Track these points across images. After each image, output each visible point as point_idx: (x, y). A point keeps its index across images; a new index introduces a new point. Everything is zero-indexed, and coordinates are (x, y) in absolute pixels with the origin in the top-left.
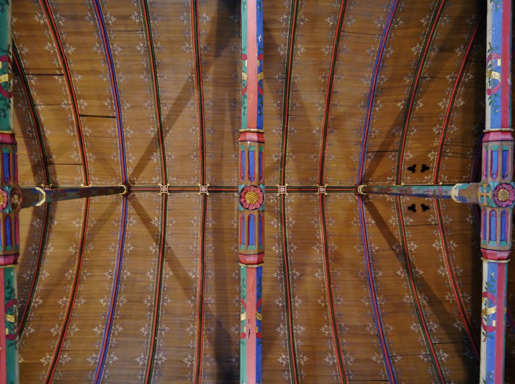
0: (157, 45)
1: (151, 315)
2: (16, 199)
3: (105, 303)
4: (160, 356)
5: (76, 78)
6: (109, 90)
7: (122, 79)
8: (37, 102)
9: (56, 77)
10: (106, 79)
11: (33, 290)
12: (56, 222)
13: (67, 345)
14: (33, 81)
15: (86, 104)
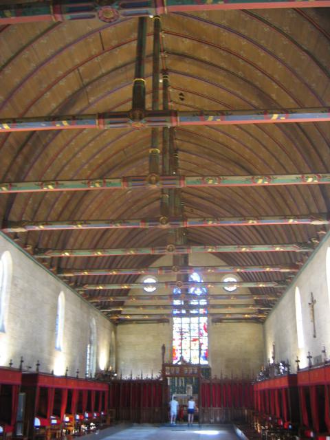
0: (38, 32)
1: (255, 21)
2: (153, 178)
3: (244, 42)
4: (286, 29)
5: (77, 61)
6: (82, 42)
7: (70, 39)
8: (100, 73)
9: (81, 71)
10: (73, 47)
11: (233, 74)
12: (186, 52)
13: (269, 72)
14: (86, 81)
15: (94, 50)
